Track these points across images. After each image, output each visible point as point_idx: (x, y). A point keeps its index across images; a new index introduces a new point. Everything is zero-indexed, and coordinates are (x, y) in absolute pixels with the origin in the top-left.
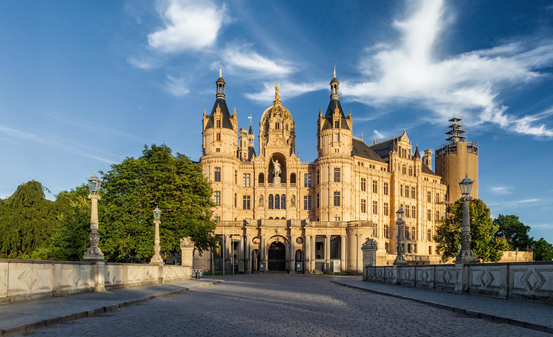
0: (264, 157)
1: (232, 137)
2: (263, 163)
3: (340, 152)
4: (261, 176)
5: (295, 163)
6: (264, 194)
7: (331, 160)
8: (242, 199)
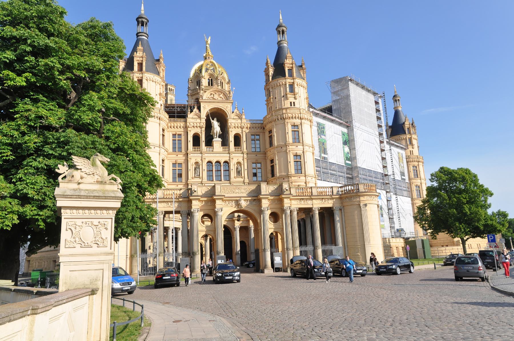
2: (199, 120)
3: (297, 105)
5: (239, 121)
6: (200, 162)
7: (287, 115)
8: (171, 168)
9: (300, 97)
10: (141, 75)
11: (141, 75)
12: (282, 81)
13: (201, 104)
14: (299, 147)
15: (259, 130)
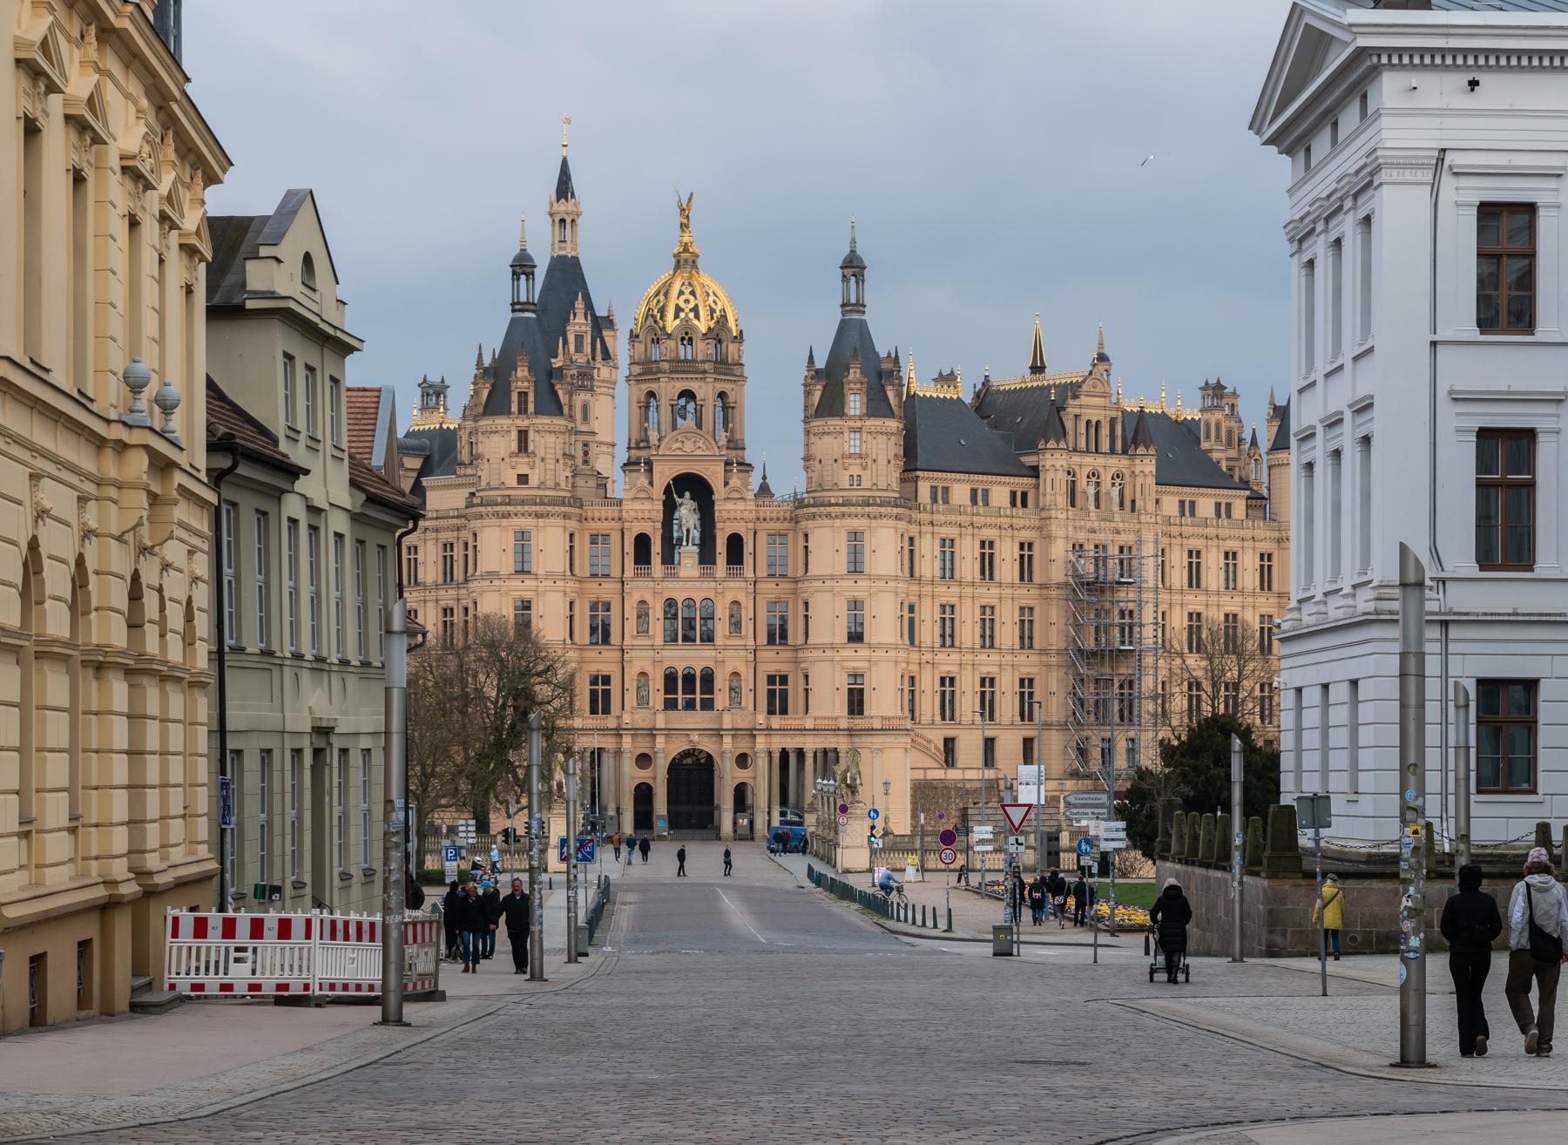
0: (650, 487)
1: (561, 436)
2: (647, 506)
3: (866, 484)
4: (642, 542)
8: (588, 613)
9: (875, 461)
10: (526, 422)
11: (526, 422)
12: (834, 422)
13: (655, 464)
14: (861, 583)
15: (786, 525)
